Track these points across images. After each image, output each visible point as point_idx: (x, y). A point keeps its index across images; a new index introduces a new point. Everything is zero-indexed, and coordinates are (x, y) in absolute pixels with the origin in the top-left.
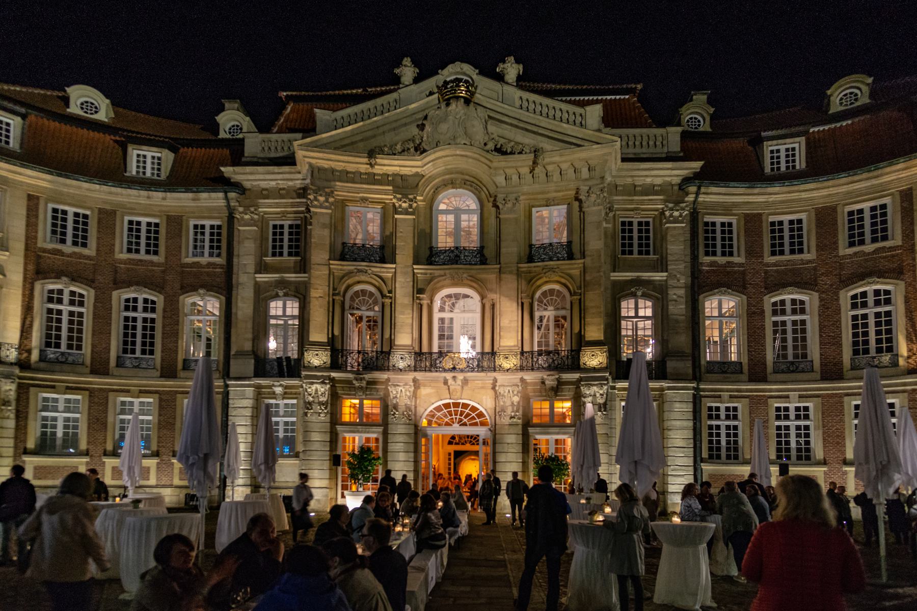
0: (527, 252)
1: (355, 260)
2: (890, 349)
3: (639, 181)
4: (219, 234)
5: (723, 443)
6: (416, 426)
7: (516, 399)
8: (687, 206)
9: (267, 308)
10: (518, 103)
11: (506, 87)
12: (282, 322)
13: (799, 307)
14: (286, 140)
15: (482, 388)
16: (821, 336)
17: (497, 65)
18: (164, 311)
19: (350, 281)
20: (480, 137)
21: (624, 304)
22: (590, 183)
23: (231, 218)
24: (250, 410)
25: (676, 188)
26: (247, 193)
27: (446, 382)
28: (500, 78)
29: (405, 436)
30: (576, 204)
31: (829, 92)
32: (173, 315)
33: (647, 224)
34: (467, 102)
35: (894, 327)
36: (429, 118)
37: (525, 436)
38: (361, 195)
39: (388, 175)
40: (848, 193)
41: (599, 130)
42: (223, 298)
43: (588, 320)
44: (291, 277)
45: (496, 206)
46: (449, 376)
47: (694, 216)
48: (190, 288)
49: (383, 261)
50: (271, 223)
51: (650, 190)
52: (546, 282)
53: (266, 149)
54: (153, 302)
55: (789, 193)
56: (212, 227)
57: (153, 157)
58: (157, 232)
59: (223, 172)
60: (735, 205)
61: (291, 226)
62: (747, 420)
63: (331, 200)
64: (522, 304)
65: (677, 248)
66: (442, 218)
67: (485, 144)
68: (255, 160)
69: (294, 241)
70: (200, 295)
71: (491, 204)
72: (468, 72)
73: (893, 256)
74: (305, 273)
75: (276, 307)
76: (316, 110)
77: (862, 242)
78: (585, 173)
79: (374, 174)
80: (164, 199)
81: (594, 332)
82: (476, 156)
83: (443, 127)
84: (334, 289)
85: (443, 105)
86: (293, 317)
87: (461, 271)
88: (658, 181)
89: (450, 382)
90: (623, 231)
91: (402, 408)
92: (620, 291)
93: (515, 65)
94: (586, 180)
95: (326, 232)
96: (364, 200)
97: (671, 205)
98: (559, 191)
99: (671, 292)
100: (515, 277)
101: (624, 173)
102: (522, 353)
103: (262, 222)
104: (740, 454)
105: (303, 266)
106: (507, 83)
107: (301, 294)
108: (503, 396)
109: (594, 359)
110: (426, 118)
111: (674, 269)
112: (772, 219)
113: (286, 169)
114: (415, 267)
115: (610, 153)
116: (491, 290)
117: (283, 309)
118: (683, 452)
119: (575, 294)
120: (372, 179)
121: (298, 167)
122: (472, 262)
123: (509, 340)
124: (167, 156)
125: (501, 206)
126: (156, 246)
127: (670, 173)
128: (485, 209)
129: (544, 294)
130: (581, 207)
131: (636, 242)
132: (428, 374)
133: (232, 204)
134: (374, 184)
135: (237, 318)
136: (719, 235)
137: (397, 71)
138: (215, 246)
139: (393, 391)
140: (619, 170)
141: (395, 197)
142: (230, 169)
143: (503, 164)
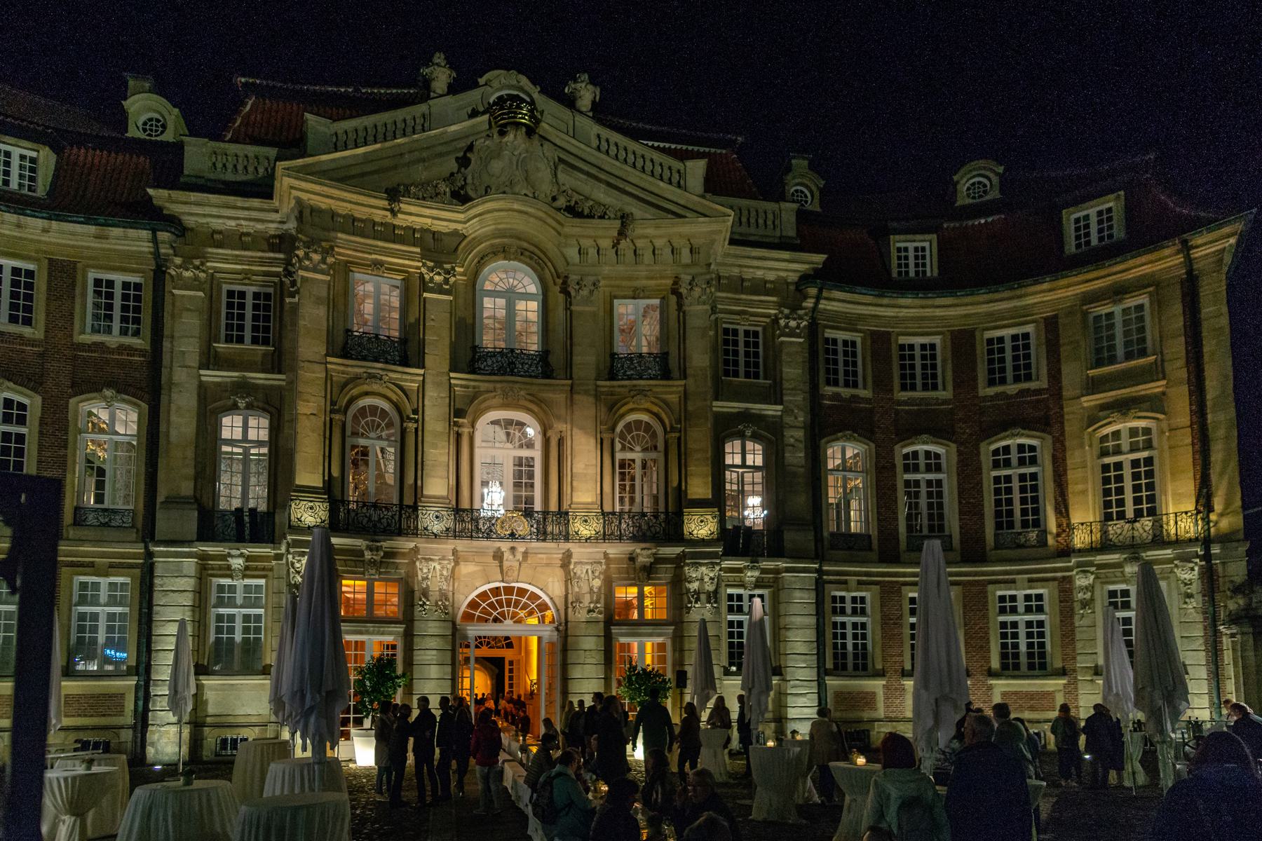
0: (608, 364)
1: (364, 359)
2: (1036, 524)
3: (748, 274)
4: (138, 299)
5: (850, 647)
6: (454, 623)
7: (597, 583)
8: (806, 314)
9: (217, 427)
10: (595, 143)
11: (578, 118)
12: (240, 450)
13: (934, 464)
14: (251, 155)
15: (548, 565)
16: (960, 502)
17: (566, 84)
18: (42, 422)
19: (355, 392)
20: (546, 188)
21: (728, 448)
22: (694, 270)
23: (160, 274)
24: (190, 595)
25: (792, 288)
26: (189, 234)
27: (498, 556)
28: (570, 102)
29: (438, 639)
30: (673, 299)
31: (955, 178)
32: (58, 429)
33: (756, 334)
34: (530, 132)
35: (1041, 494)
36: (475, 149)
37: (608, 639)
38: (374, 256)
39: (415, 230)
40: (990, 314)
41: (703, 197)
42: (145, 406)
43: (692, 469)
44: (258, 378)
45: (565, 291)
46: (505, 546)
47: (813, 331)
48: (88, 386)
49: (405, 362)
50: (225, 287)
51: (760, 287)
52: (632, 410)
53: (219, 165)
54: (22, 407)
55: (923, 307)
56: (126, 285)
57: (22, 157)
58: (29, 286)
59: (150, 198)
60: (861, 317)
61: (256, 296)
62: (878, 617)
63: (330, 260)
64: (602, 440)
65: (793, 372)
66: (488, 302)
67: (554, 199)
68: (201, 182)
69: (259, 322)
70: (105, 398)
71: (558, 288)
72: (526, 88)
73: (1038, 401)
74: (280, 372)
75: (231, 426)
76: (307, 115)
77: (1003, 381)
78: (686, 257)
79: (394, 226)
80: (45, 231)
81: (699, 488)
82: (541, 214)
83: (496, 166)
84: (333, 403)
85: (495, 131)
86: (259, 444)
87: (517, 386)
88: (771, 276)
89: (507, 555)
90: (726, 342)
91: (434, 596)
92: (726, 428)
93: (590, 87)
94: (687, 266)
95: (322, 311)
96: (377, 264)
97: (786, 311)
98: (652, 278)
99: (788, 433)
100: (592, 400)
101: (730, 260)
102: (603, 513)
103: (212, 285)
104: (1048, 659)
105: (278, 362)
106: (581, 112)
107: (276, 407)
108: (579, 578)
109: (701, 526)
110: (470, 148)
111: (790, 401)
112: (903, 340)
113: (256, 202)
114: (452, 375)
115: (720, 231)
116: (558, 418)
117: (242, 430)
118: (805, 661)
119: (673, 429)
120: (390, 234)
121: (276, 203)
122: (533, 373)
123: (584, 494)
124: (46, 158)
125: (573, 294)
126: (28, 309)
127: (784, 267)
128: (550, 294)
129: (628, 427)
130: (680, 306)
131: (742, 359)
132: (475, 543)
133: (162, 251)
134: (394, 242)
135: (168, 442)
136: (918, 362)
137: (425, 71)
138: (131, 319)
139: (423, 569)
140: (727, 255)
141: (424, 265)
142: (164, 193)
143: (576, 230)
